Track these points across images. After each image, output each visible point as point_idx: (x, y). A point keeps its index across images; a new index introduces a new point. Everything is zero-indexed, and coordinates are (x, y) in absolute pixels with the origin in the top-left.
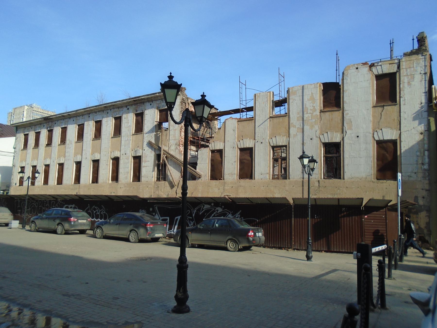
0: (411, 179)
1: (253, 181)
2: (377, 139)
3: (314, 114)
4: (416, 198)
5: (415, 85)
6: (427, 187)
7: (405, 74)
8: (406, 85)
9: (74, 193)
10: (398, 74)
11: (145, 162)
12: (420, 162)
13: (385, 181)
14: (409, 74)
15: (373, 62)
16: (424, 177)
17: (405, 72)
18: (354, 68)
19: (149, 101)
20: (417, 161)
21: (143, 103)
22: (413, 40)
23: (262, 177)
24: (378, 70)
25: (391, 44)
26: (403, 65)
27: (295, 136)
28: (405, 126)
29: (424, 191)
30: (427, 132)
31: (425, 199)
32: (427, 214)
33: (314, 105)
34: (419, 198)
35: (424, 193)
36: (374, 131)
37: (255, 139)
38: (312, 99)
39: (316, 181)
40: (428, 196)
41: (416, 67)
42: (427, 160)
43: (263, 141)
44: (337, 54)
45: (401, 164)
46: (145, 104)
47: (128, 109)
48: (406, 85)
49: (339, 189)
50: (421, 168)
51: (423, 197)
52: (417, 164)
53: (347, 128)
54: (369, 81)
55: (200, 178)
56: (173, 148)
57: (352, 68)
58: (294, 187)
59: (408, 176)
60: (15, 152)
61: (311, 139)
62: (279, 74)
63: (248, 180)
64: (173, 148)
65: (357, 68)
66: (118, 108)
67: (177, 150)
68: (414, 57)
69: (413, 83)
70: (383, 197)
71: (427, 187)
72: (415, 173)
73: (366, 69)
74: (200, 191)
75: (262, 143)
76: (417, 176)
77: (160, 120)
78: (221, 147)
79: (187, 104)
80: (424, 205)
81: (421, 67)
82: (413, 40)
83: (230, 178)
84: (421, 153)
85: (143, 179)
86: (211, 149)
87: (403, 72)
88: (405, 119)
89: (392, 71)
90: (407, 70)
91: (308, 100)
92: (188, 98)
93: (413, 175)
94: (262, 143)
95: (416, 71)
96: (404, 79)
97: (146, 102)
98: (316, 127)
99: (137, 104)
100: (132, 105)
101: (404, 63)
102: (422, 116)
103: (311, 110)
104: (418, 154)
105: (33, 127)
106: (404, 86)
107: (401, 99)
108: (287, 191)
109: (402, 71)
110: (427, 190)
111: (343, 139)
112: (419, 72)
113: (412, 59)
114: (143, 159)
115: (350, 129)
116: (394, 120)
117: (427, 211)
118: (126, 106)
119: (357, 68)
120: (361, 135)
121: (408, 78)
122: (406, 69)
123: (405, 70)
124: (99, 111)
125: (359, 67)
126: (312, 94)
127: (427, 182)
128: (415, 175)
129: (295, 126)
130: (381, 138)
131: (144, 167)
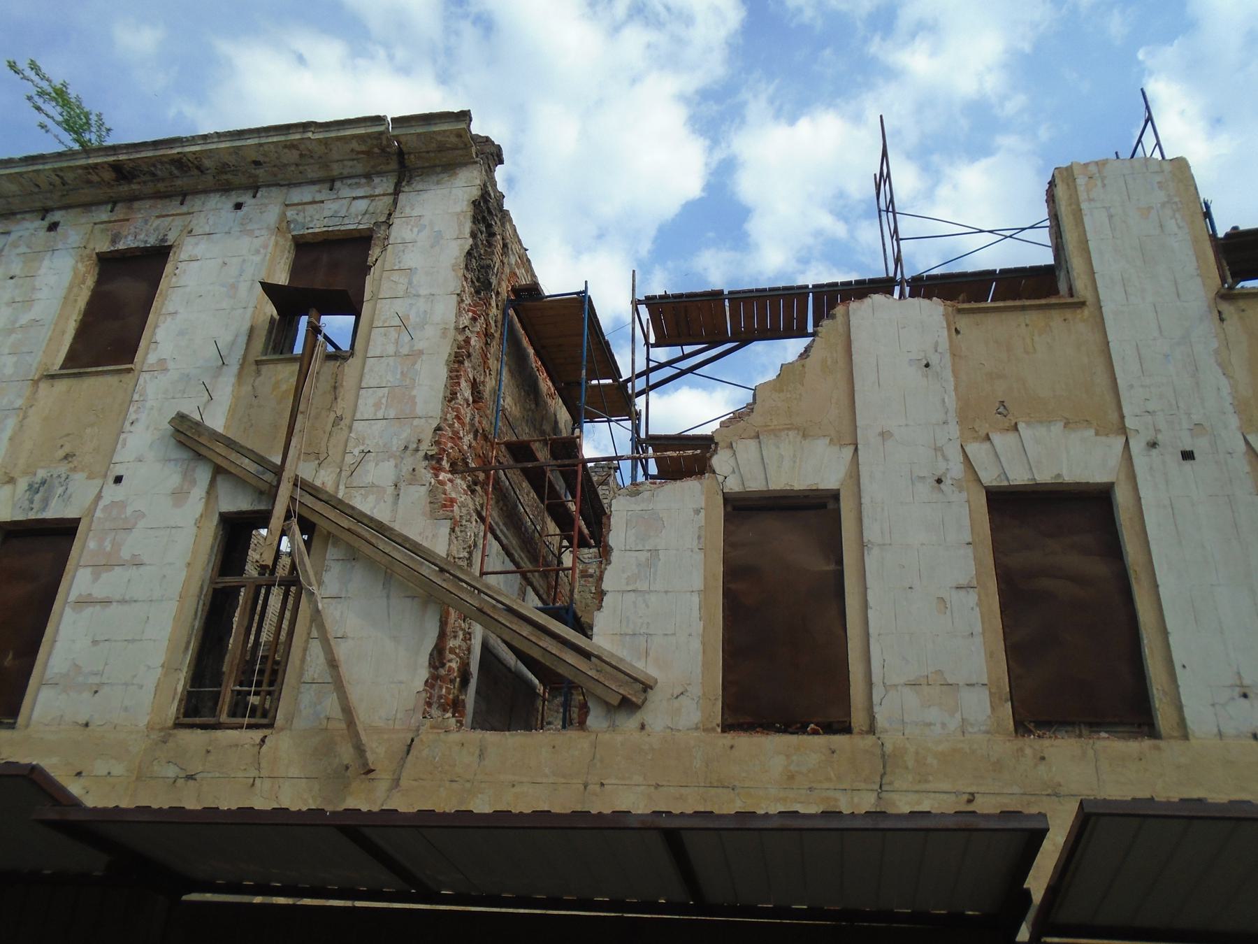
1: (1171, 750)
11: (104, 565)
19: (225, 188)
37: (1123, 430)
43: (1199, 445)
55: (627, 705)
67: (417, 495)
78: (830, 481)
83: (933, 714)
86: (733, 485)
94: (1188, 456)
97: (206, 192)
99: (132, 199)
100: (87, 206)
114: (86, 547)
131: (85, 602)
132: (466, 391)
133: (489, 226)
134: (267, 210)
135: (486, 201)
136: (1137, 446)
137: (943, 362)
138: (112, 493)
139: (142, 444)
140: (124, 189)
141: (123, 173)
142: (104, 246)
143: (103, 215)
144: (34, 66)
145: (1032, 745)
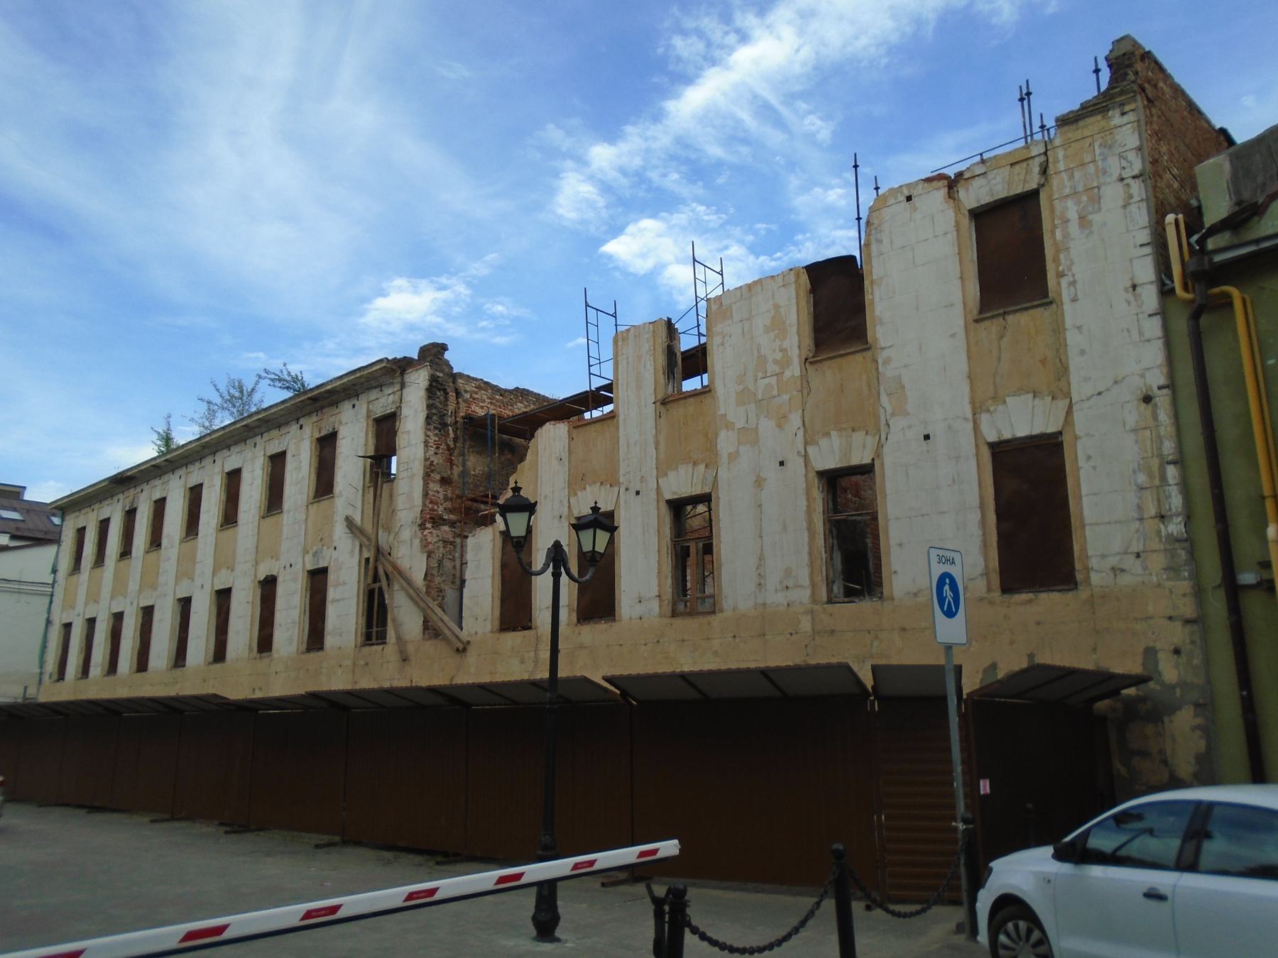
0: (1125, 580)
1: (616, 627)
2: (992, 437)
3: (788, 374)
4: (1150, 653)
5: (1105, 224)
6: (1189, 610)
7: (1067, 191)
8: (1074, 228)
9: (172, 693)
10: (1043, 196)
12: (1153, 512)
13: (1031, 595)
14: (1080, 189)
15: (962, 167)
16: (1172, 570)
17: (1068, 184)
18: (902, 198)
19: (349, 397)
20: (1139, 507)
21: (335, 404)
22: (1097, 71)
23: (639, 610)
24: (976, 195)
25: (1022, 100)
26: (1060, 160)
27: (733, 457)
28: (1087, 379)
29: (1178, 624)
30: (1165, 391)
31: (1184, 659)
32: (1198, 721)
33: (786, 344)
34: (1161, 655)
35: (1179, 635)
36: (978, 408)
38: (777, 325)
39: (806, 613)
40: (1193, 642)
41: (1104, 160)
42: (1176, 501)
44: (856, 166)
45: (1083, 526)
46: (340, 405)
47: (301, 427)
48: (1074, 228)
49: (877, 637)
50: (1159, 532)
51: (1177, 651)
52: (1141, 519)
53: (889, 410)
54: (949, 236)
56: (406, 534)
57: (892, 201)
58: (737, 640)
59: (1113, 569)
60: (54, 581)
61: (782, 463)
62: (694, 260)
63: (602, 626)
64: (406, 534)
65: (909, 198)
66: (279, 427)
67: (417, 542)
68: (1093, 125)
69: (1096, 218)
70: (1031, 656)
71: (1189, 610)
72: (1138, 556)
73: (940, 194)
74: (472, 669)
75: (638, 493)
76: (1145, 568)
77: (377, 450)
79: (452, 394)
80: (1182, 684)
81: (1121, 156)
82: (1097, 71)
84: (1151, 476)
85: (329, 641)
87: (1061, 183)
88: (1083, 352)
89: (1018, 189)
90: (1072, 177)
91: (768, 330)
92: (455, 377)
93: (1130, 562)
95: (1105, 172)
96: (1067, 208)
98: (795, 420)
99: (322, 408)
100: (309, 414)
101: (1061, 154)
102: (1141, 333)
103: (776, 362)
104: (1142, 478)
105: (96, 506)
106: (1066, 236)
107: (1064, 282)
108: (716, 653)
109: (1055, 182)
110: (1188, 622)
111: (878, 452)
112: (1115, 176)
113: (1087, 132)
114: (331, 577)
115: (901, 411)
116: (1043, 362)
117: (1197, 705)
118: (298, 420)
119: (909, 198)
120: (937, 430)
121: (1078, 203)
122: (1071, 172)
123: (1065, 176)
124: (236, 443)
125: (914, 193)
126: (777, 307)
127: (1185, 586)
128: (1138, 562)
129: (729, 426)
130: (1007, 435)
132: (434, 487)
133: (445, 390)
134: (362, 405)
135: (437, 381)
136: (622, 490)
137: (565, 457)
138: (335, 554)
139: (340, 530)
140: (318, 404)
141: (314, 399)
142: (317, 435)
143: (314, 418)
144: (266, 371)
145: (579, 627)
